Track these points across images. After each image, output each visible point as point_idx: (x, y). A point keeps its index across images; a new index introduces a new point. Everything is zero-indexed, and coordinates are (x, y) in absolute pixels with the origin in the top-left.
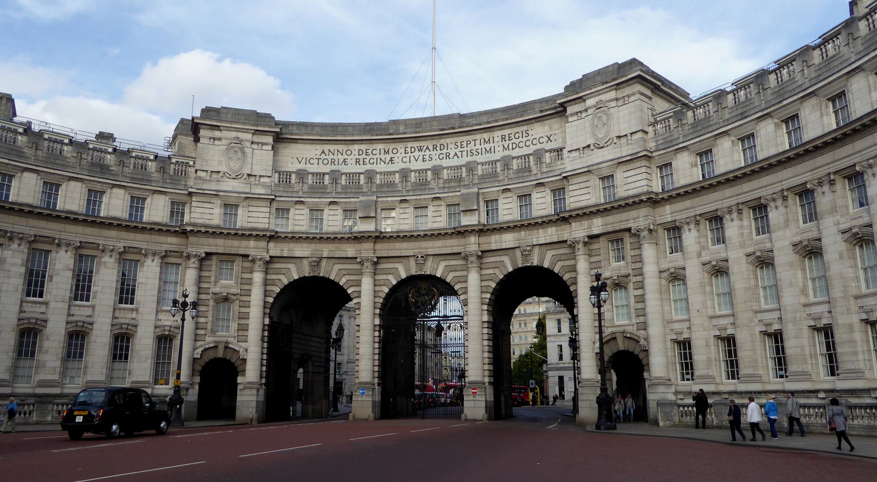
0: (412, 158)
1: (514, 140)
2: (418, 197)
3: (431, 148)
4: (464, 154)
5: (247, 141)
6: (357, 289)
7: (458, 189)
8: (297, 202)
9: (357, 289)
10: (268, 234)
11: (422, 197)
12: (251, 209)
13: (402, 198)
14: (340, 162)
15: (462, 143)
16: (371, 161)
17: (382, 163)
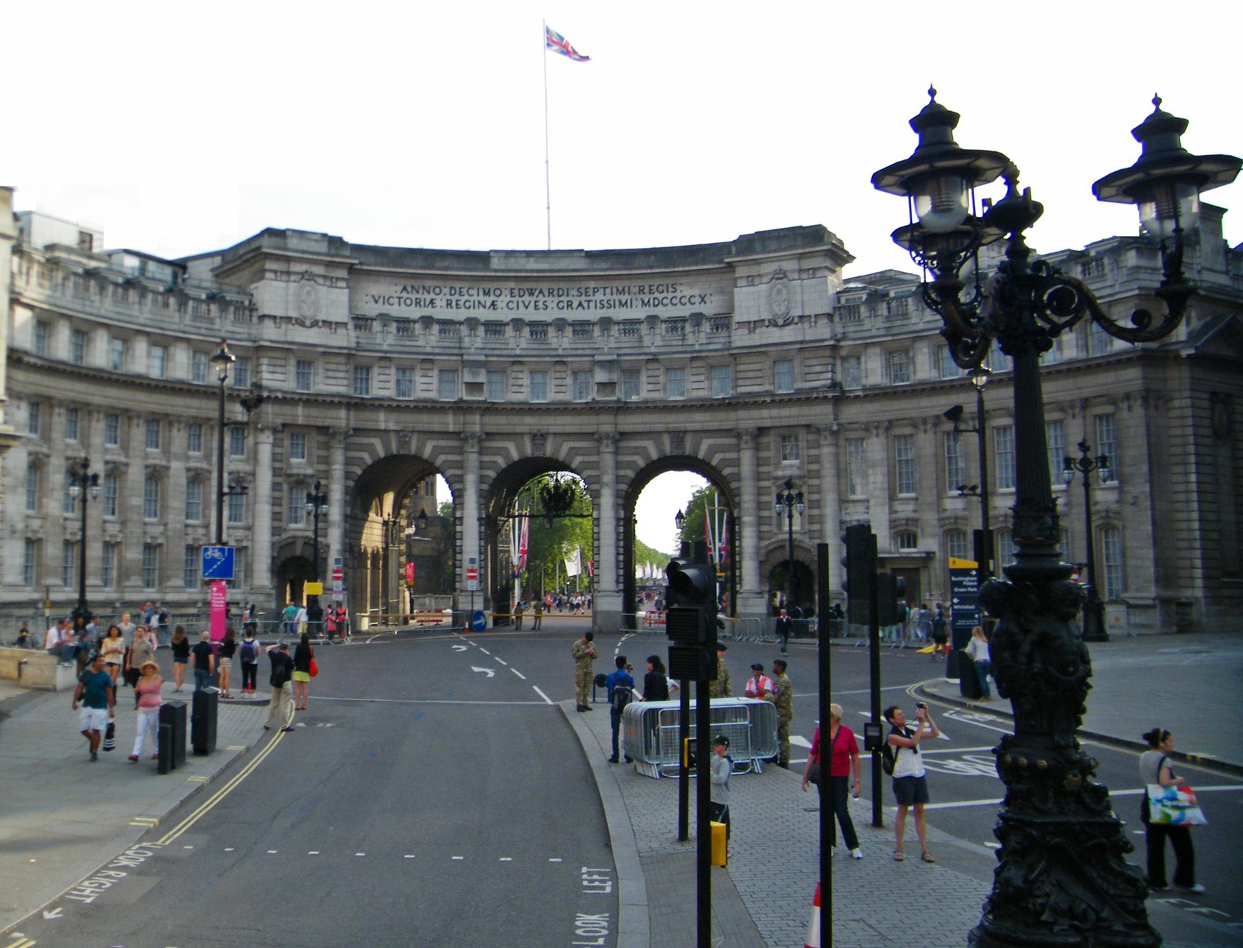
0: (521, 305)
1: (656, 295)
5: (319, 276)
6: (458, 472)
7: (587, 352)
8: (381, 358)
9: (458, 472)
10: (353, 401)
12: (329, 366)
14: (428, 301)
16: (467, 304)
17: (481, 308)
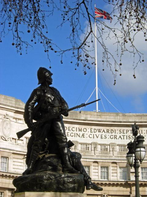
0: (95, 136)
2: (104, 161)
3: (106, 131)
4: (125, 137)
5: (11, 117)
11: (106, 161)
13: (95, 160)
15: (124, 131)
16: (72, 135)
